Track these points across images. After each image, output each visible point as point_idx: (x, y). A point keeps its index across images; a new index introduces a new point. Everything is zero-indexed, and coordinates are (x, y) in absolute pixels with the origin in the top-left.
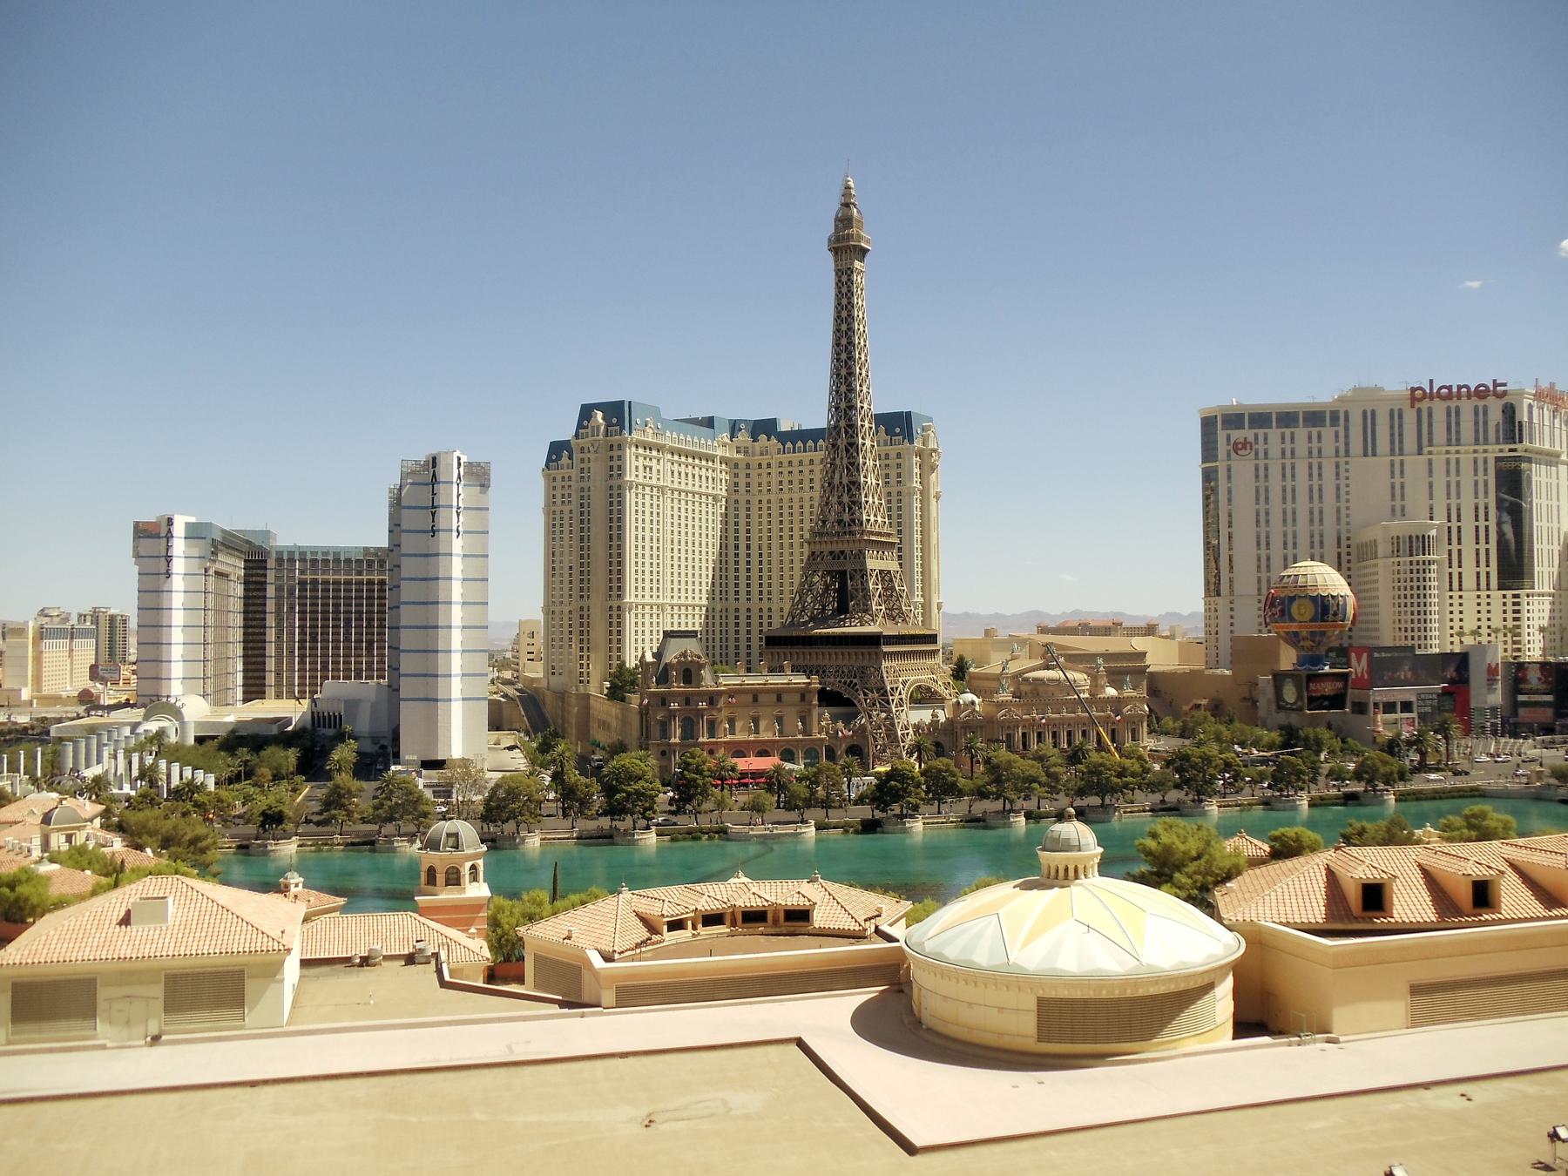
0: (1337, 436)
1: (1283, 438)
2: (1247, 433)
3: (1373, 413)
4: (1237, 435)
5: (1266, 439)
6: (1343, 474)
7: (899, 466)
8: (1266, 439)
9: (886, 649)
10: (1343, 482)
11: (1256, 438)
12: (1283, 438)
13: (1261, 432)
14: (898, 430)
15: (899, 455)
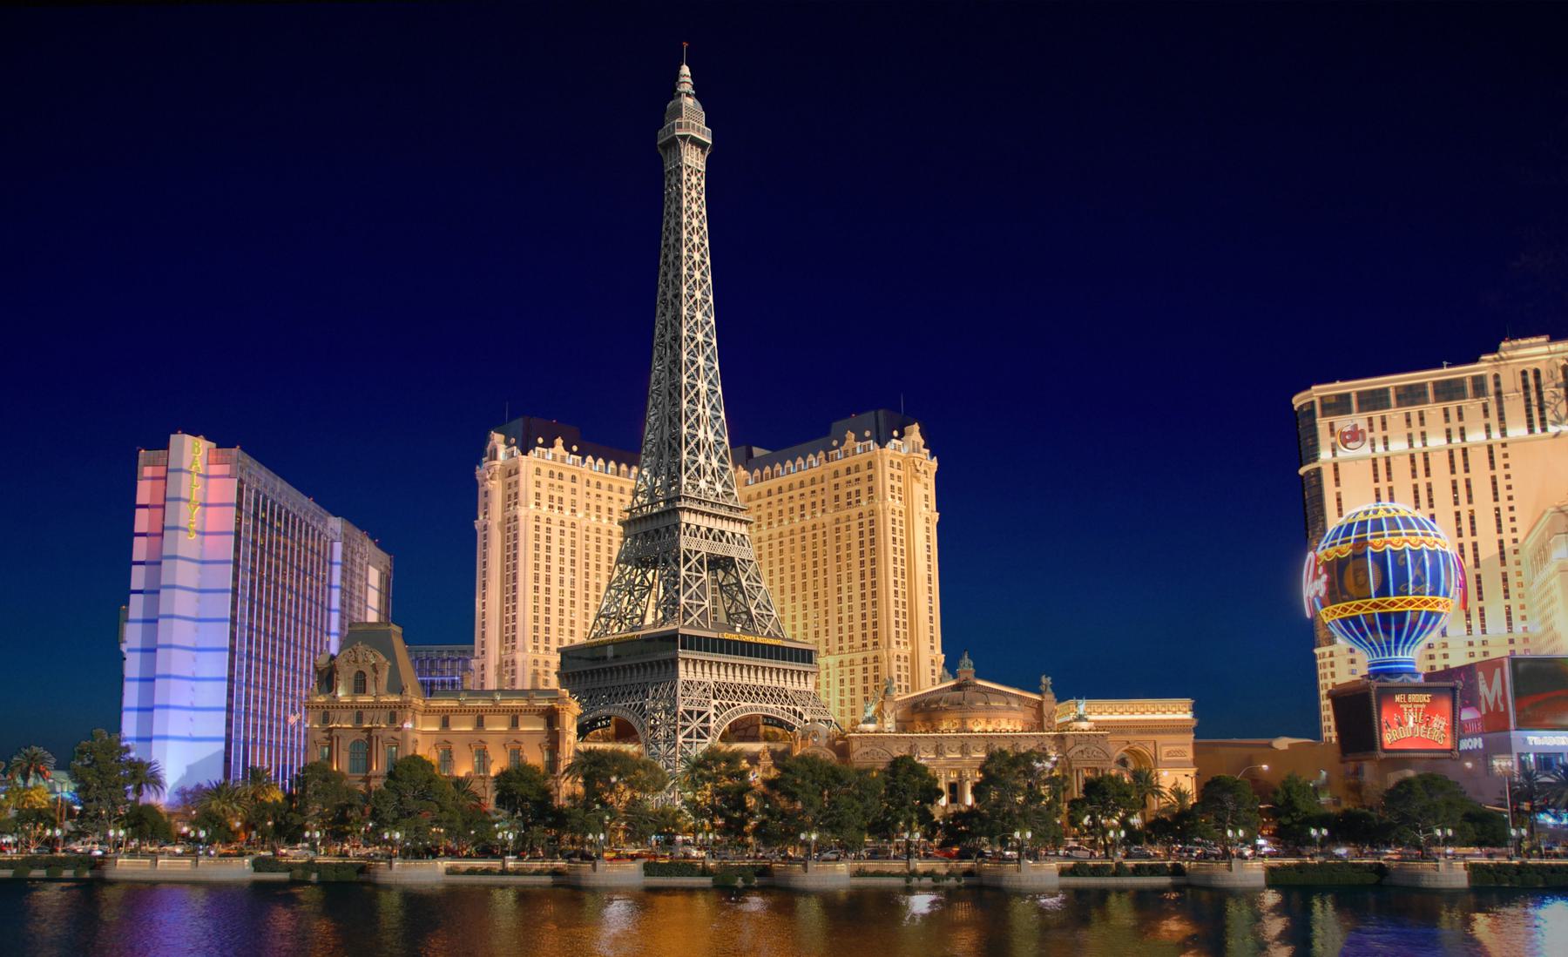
0: (1486, 412)
1: (1408, 421)
2: (1358, 419)
3: (1537, 373)
4: (1343, 423)
5: (1384, 424)
6: (1499, 461)
7: (870, 478)
8: (1384, 424)
9: (681, 653)
10: (1500, 472)
11: (1371, 425)
12: (1408, 421)
13: (1376, 415)
14: (867, 434)
15: (870, 465)
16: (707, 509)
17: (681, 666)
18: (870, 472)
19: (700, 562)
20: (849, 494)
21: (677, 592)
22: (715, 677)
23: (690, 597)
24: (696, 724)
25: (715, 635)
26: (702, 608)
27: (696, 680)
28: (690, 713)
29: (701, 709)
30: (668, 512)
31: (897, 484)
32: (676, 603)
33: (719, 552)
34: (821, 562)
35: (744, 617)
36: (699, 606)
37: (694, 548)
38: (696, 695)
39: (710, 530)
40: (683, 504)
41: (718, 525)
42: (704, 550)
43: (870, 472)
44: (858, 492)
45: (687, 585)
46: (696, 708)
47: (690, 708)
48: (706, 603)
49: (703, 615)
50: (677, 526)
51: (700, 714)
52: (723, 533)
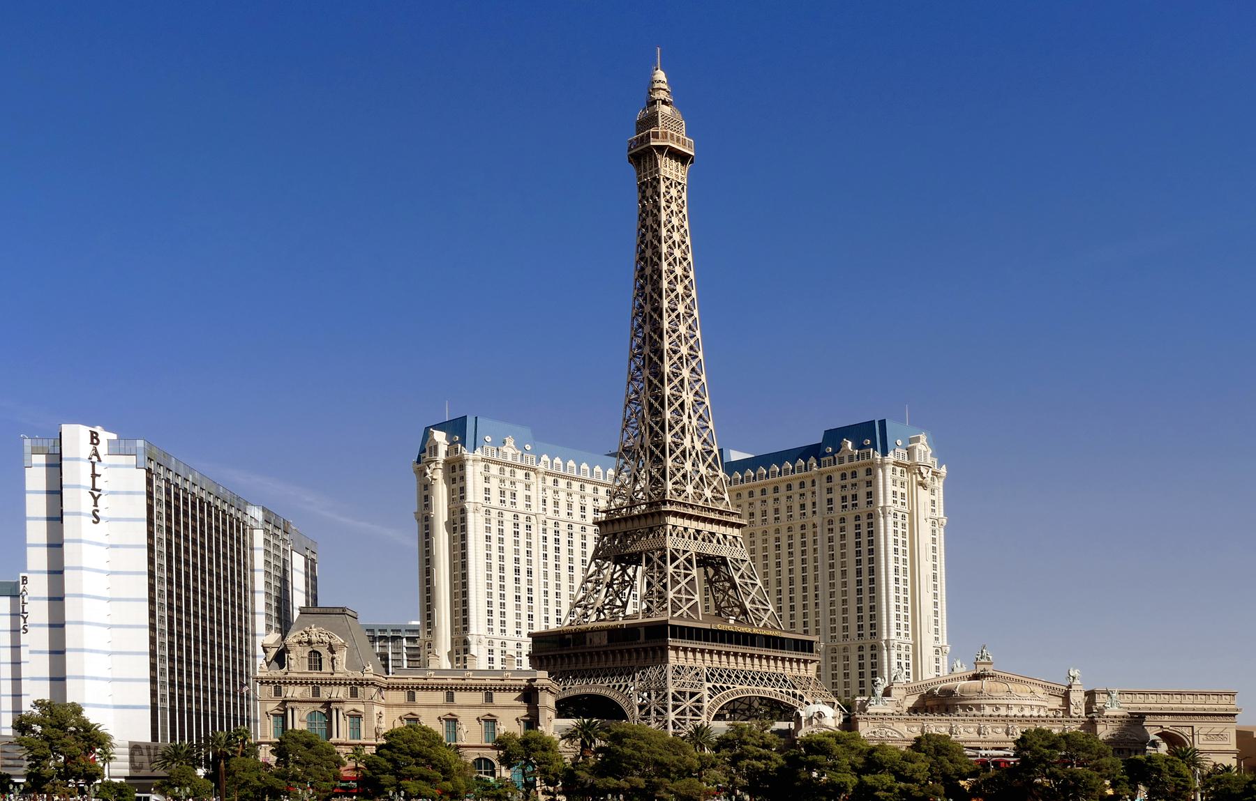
16: (695, 512)
17: (672, 654)
18: (869, 478)
19: (689, 561)
20: (844, 499)
21: (665, 586)
22: (708, 663)
23: (679, 592)
24: (688, 703)
25: (707, 626)
26: (690, 602)
27: (687, 665)
28: (682, 693)
29: (693, 690)
30: (652, 515)
31: (900, 490)
32: (662, 597)
33: (710, 550)
34: (811, 578)
35: (737, 610)
36: (688, 600)
37: (681, 547)
38: (688, 678)
39: (698, 532)
40: (668, 508)
41: (707, 528)
42: (694, 548)
43: (869, 478)
44: (855, 497)
45: (675, 582)
46: (688, 690)
47: (683, 689)
48: (697, 598)
49: (694, 608)
50: (664, 525)
51: (692, 695)
52: (713, 534)
